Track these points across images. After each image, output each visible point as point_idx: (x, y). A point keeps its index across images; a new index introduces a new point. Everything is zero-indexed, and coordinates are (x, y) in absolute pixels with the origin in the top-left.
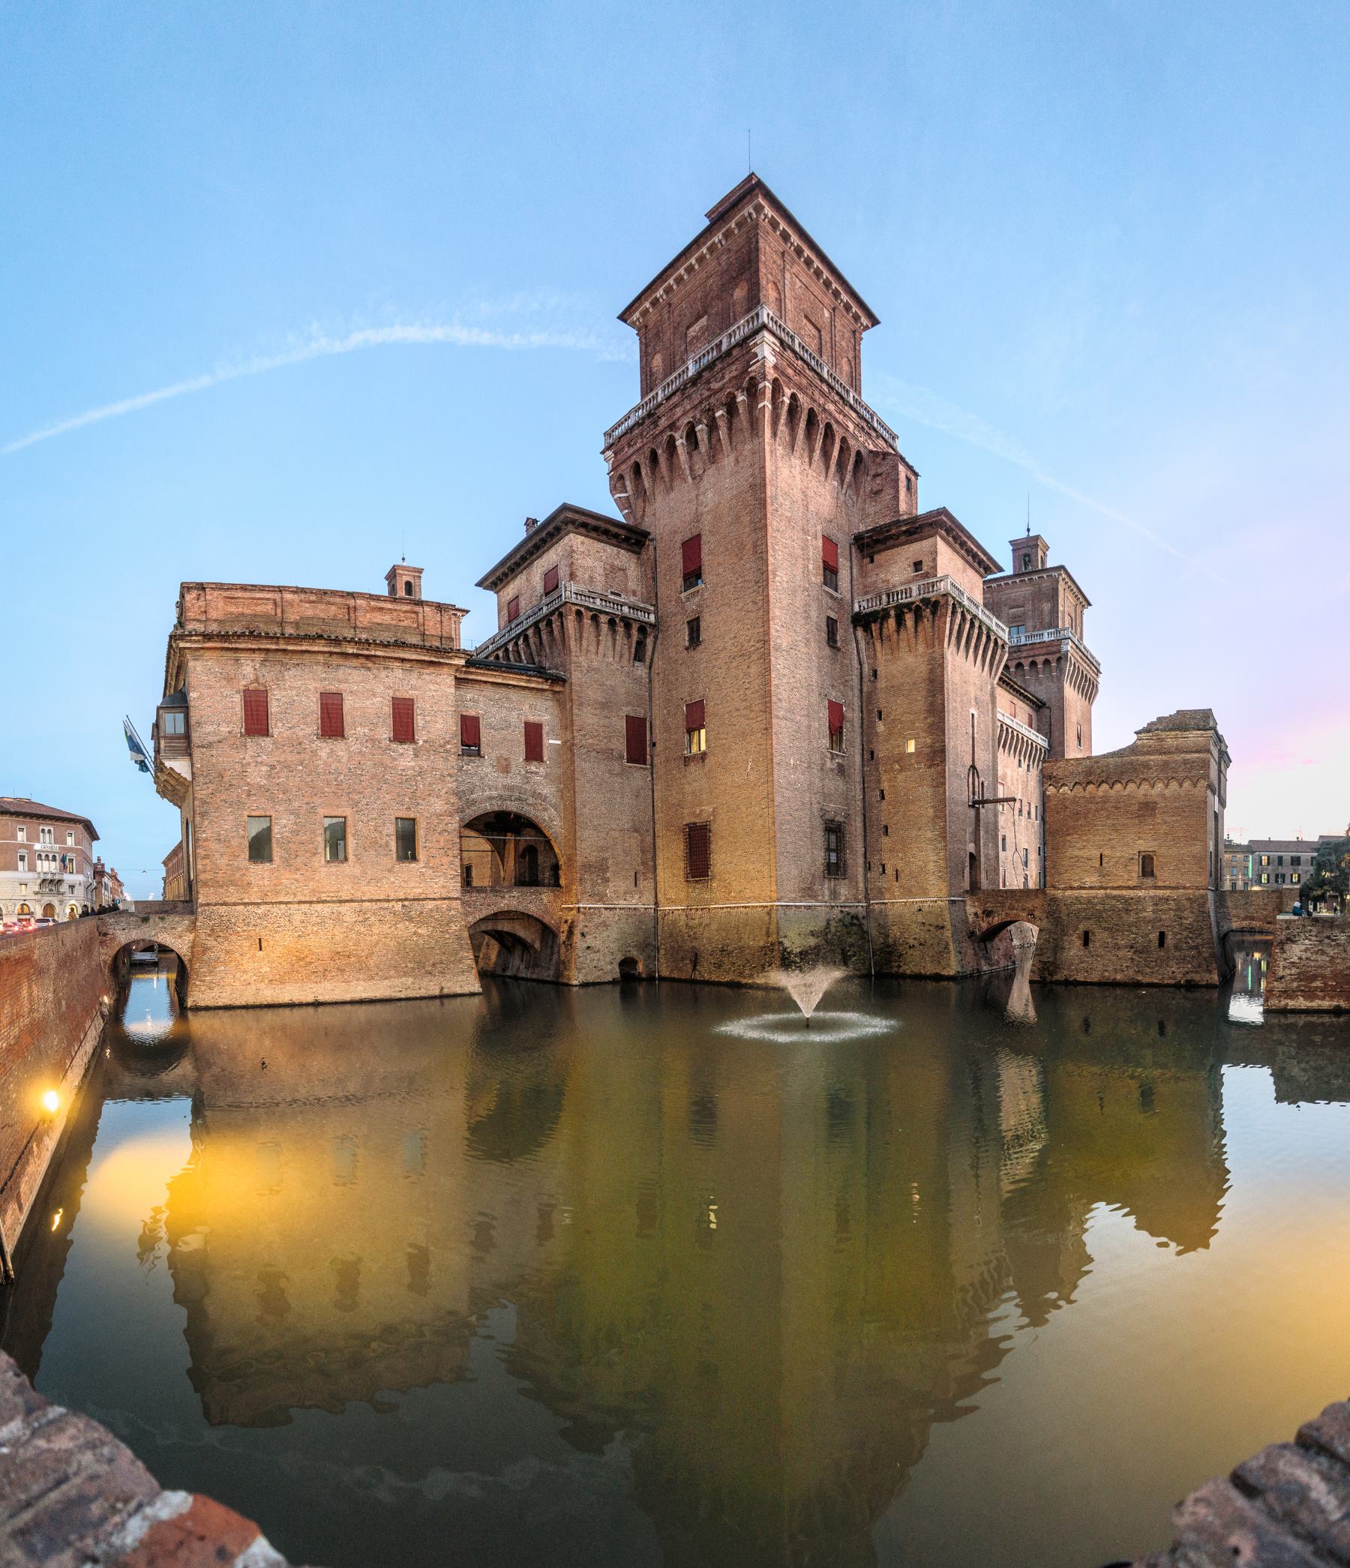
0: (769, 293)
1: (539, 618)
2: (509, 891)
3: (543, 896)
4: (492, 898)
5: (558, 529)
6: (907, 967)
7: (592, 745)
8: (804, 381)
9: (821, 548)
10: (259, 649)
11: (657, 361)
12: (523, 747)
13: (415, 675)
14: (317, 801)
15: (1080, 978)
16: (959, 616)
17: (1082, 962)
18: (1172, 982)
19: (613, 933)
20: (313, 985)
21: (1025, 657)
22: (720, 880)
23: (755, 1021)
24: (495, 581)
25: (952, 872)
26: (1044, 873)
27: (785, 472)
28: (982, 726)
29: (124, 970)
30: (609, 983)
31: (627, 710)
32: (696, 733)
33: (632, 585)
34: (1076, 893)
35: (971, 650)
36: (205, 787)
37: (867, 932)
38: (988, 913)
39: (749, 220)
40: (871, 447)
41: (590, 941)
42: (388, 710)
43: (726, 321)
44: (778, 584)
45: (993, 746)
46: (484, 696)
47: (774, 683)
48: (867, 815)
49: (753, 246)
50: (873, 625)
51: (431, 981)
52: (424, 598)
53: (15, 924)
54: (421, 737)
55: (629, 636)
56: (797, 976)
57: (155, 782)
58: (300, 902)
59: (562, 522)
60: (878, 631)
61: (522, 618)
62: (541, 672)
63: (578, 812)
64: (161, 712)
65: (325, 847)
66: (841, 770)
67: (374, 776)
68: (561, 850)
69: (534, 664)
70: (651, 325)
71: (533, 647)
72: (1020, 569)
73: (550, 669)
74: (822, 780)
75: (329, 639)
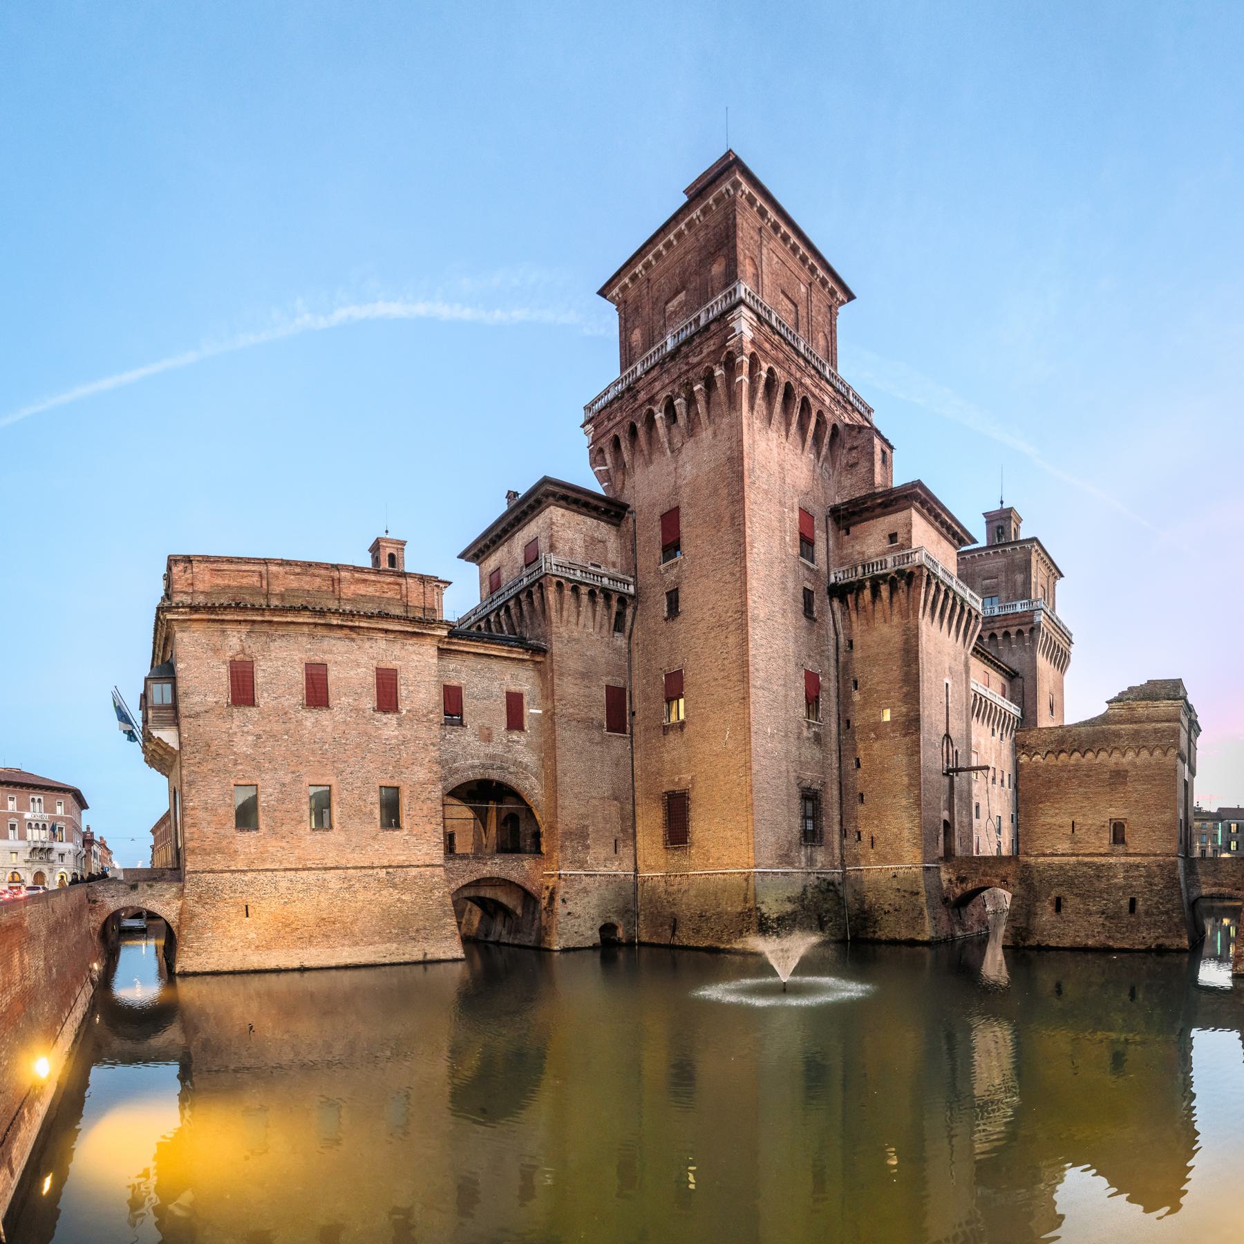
0: (746, 268)
1: (519, 589)
2: (492, 858)
3: (525, 863)
4: (474, 865)
5: (539, 502)
6: (883, 932)
7: (572, 714)
8: (781, 356)
9: (797, 520)
10: (245, 621)
11: (636, 336)
12: (505, 717)
13: (398, 646)
14: (303, 770)
15: (1052, 943)
16: (933, 587)
17: (1054, 928)
18: (1142, 947)
19: (594, 899)
20: (298, 951)
21: (998, 628)
22: (699, 847)
23: (733, 985)
24: (477, 552)
25: (926, 838)
26: (1017, 839)
27: (762, 445)
28: (956, 695)
29: (113, 937)
30: (589, 948)
31: (606, 680)
32: (675, 703)
33: (612, 556)
34: (1049, 860)
35: (946, 621)
36: (192, 756)
37: (843, 898)
38: (962, 880)
39: (726, 196)
40: (847, 421)
41: (571, 906)
42: (372, 680)
43: (703, 296)
44: (756, 556)
45: (967, 716)
47: (751, 653)
48: (843, 783)
49: (730, 222)
50: (849, 596)
51: (415, 947)
52: (407, 570)
53: (6, 892)
54: (404, 707)
56: (774, 941)
57: (143, 752)
58: (286, 870)
59: (543, 495)
60: (854, 602)
61: (504, 589)
62: (521, 643)
63: (559, 781)
64: (149, 682)
65: (311, 815)
66: (818, 739)
67: (358, 745)
68: (542, 818)
69: (516, 634)
70: (630, 301)
71: (514, 618)
72: (994, 540)
73: (531, 639)
74: (799, 748)
75: (314, 611)
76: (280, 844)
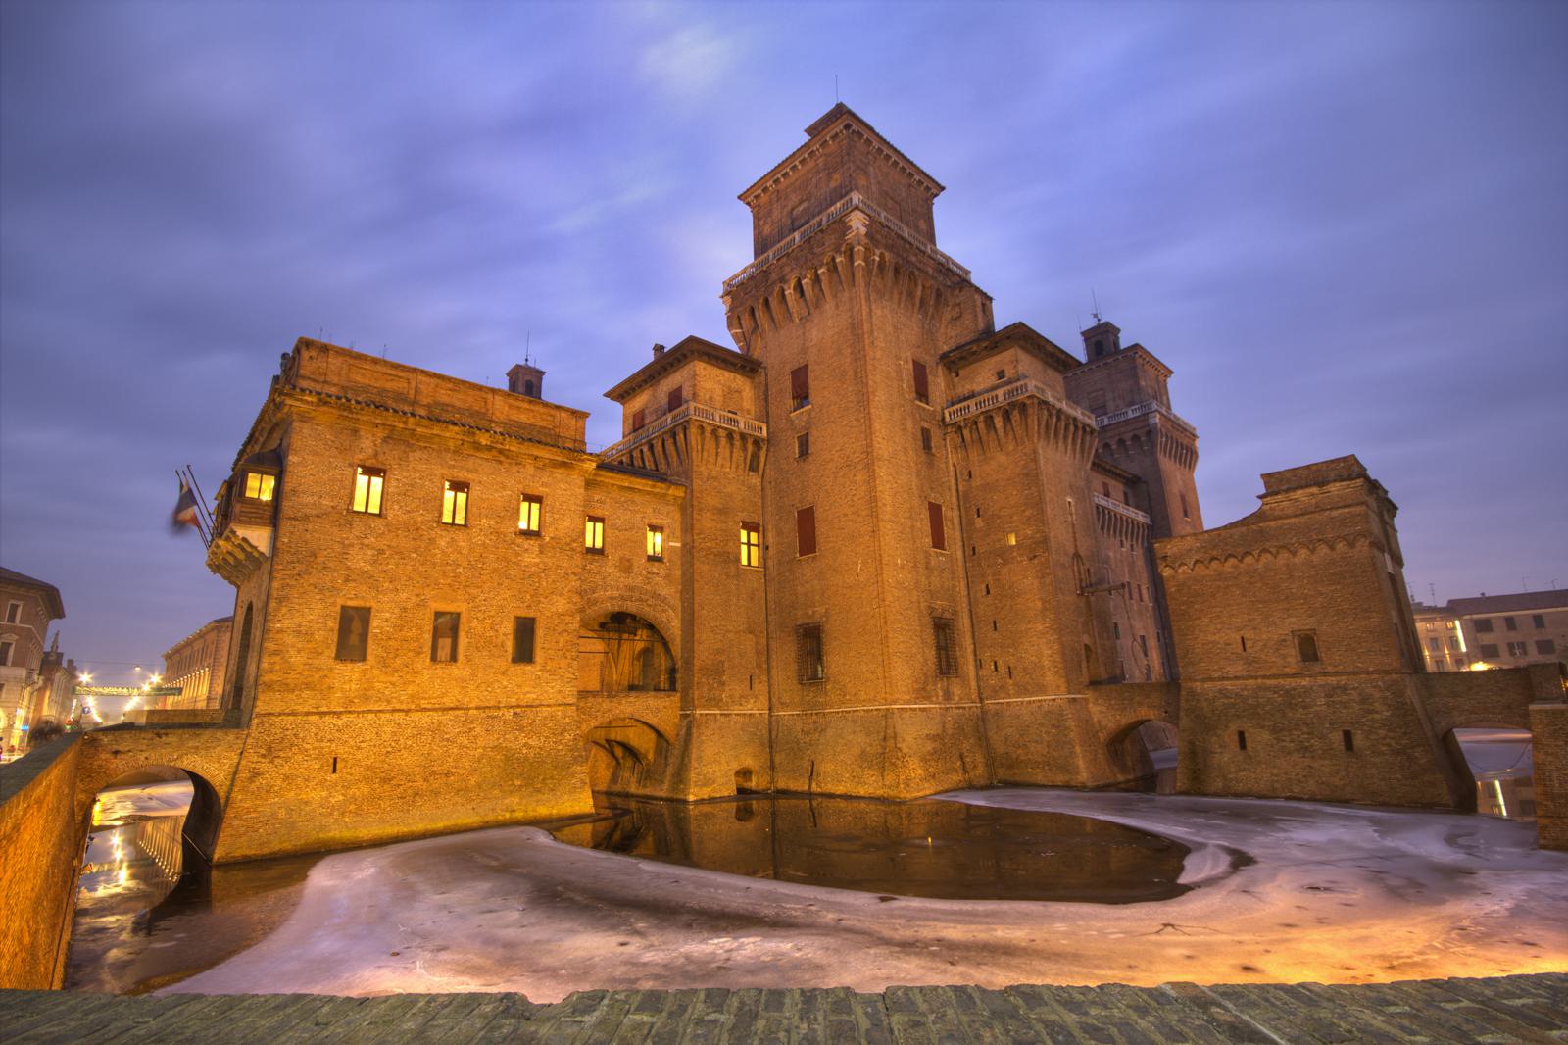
7: (709, 548)
14: (429, 593)
24: (622, 393)
46: (611, 498)
55: (745, 449)
58: (394, 710)
67: (495, 570)
74: (928, 578)
76: (390, 679)
